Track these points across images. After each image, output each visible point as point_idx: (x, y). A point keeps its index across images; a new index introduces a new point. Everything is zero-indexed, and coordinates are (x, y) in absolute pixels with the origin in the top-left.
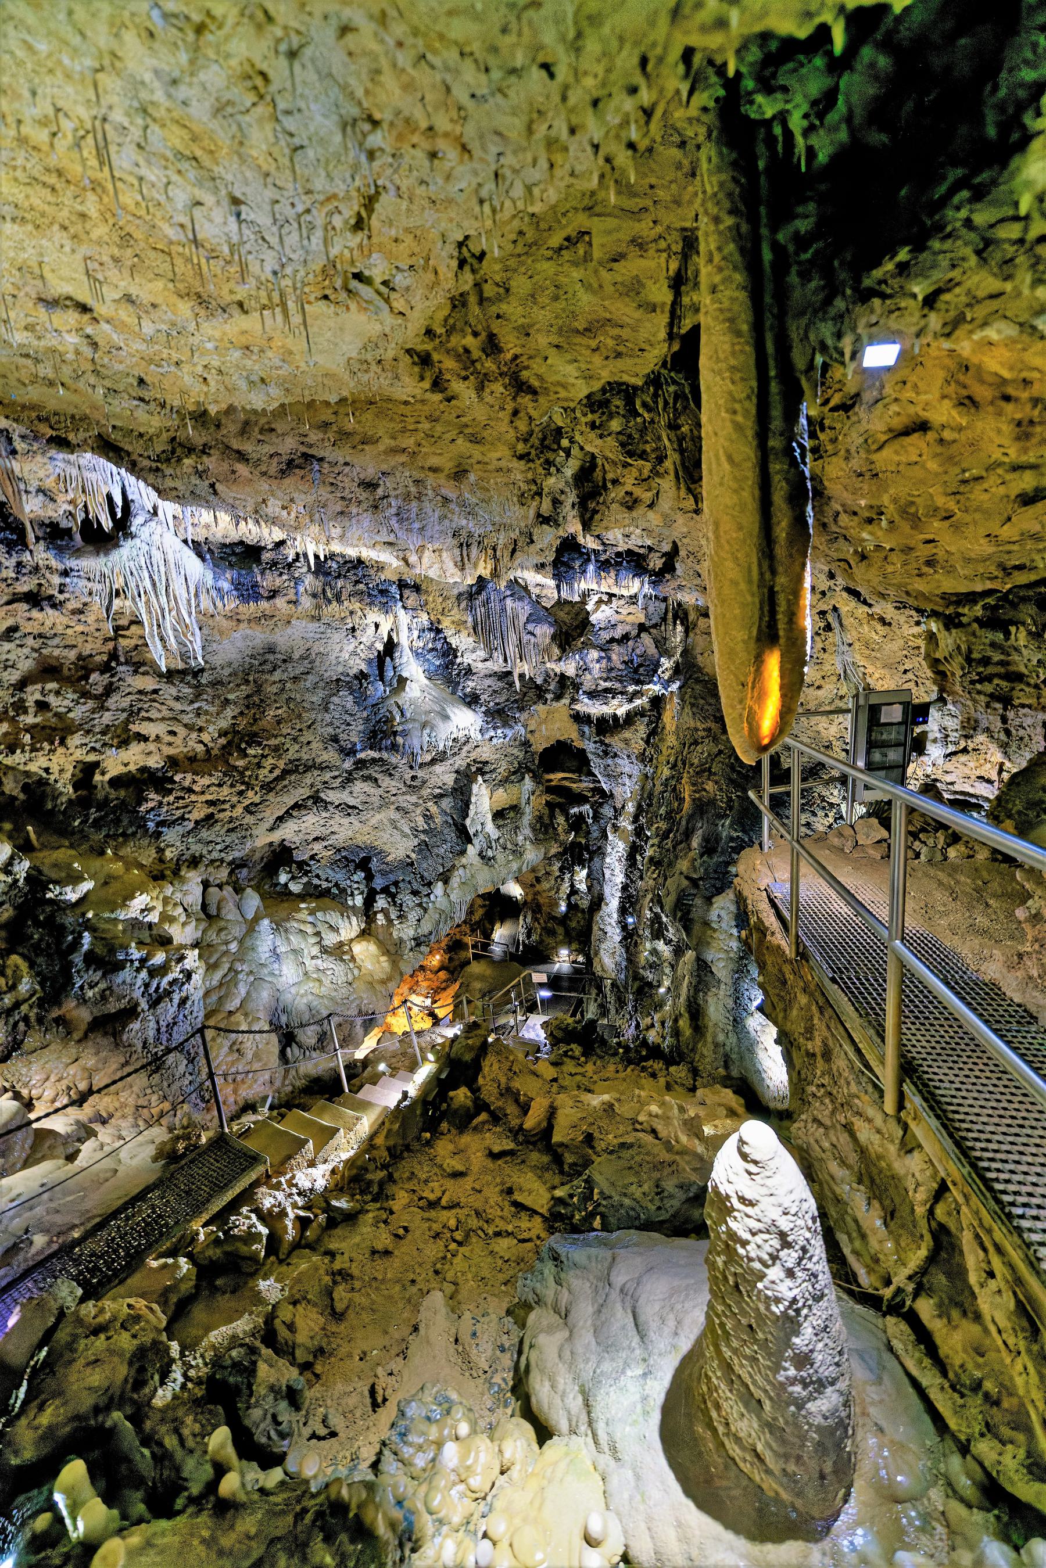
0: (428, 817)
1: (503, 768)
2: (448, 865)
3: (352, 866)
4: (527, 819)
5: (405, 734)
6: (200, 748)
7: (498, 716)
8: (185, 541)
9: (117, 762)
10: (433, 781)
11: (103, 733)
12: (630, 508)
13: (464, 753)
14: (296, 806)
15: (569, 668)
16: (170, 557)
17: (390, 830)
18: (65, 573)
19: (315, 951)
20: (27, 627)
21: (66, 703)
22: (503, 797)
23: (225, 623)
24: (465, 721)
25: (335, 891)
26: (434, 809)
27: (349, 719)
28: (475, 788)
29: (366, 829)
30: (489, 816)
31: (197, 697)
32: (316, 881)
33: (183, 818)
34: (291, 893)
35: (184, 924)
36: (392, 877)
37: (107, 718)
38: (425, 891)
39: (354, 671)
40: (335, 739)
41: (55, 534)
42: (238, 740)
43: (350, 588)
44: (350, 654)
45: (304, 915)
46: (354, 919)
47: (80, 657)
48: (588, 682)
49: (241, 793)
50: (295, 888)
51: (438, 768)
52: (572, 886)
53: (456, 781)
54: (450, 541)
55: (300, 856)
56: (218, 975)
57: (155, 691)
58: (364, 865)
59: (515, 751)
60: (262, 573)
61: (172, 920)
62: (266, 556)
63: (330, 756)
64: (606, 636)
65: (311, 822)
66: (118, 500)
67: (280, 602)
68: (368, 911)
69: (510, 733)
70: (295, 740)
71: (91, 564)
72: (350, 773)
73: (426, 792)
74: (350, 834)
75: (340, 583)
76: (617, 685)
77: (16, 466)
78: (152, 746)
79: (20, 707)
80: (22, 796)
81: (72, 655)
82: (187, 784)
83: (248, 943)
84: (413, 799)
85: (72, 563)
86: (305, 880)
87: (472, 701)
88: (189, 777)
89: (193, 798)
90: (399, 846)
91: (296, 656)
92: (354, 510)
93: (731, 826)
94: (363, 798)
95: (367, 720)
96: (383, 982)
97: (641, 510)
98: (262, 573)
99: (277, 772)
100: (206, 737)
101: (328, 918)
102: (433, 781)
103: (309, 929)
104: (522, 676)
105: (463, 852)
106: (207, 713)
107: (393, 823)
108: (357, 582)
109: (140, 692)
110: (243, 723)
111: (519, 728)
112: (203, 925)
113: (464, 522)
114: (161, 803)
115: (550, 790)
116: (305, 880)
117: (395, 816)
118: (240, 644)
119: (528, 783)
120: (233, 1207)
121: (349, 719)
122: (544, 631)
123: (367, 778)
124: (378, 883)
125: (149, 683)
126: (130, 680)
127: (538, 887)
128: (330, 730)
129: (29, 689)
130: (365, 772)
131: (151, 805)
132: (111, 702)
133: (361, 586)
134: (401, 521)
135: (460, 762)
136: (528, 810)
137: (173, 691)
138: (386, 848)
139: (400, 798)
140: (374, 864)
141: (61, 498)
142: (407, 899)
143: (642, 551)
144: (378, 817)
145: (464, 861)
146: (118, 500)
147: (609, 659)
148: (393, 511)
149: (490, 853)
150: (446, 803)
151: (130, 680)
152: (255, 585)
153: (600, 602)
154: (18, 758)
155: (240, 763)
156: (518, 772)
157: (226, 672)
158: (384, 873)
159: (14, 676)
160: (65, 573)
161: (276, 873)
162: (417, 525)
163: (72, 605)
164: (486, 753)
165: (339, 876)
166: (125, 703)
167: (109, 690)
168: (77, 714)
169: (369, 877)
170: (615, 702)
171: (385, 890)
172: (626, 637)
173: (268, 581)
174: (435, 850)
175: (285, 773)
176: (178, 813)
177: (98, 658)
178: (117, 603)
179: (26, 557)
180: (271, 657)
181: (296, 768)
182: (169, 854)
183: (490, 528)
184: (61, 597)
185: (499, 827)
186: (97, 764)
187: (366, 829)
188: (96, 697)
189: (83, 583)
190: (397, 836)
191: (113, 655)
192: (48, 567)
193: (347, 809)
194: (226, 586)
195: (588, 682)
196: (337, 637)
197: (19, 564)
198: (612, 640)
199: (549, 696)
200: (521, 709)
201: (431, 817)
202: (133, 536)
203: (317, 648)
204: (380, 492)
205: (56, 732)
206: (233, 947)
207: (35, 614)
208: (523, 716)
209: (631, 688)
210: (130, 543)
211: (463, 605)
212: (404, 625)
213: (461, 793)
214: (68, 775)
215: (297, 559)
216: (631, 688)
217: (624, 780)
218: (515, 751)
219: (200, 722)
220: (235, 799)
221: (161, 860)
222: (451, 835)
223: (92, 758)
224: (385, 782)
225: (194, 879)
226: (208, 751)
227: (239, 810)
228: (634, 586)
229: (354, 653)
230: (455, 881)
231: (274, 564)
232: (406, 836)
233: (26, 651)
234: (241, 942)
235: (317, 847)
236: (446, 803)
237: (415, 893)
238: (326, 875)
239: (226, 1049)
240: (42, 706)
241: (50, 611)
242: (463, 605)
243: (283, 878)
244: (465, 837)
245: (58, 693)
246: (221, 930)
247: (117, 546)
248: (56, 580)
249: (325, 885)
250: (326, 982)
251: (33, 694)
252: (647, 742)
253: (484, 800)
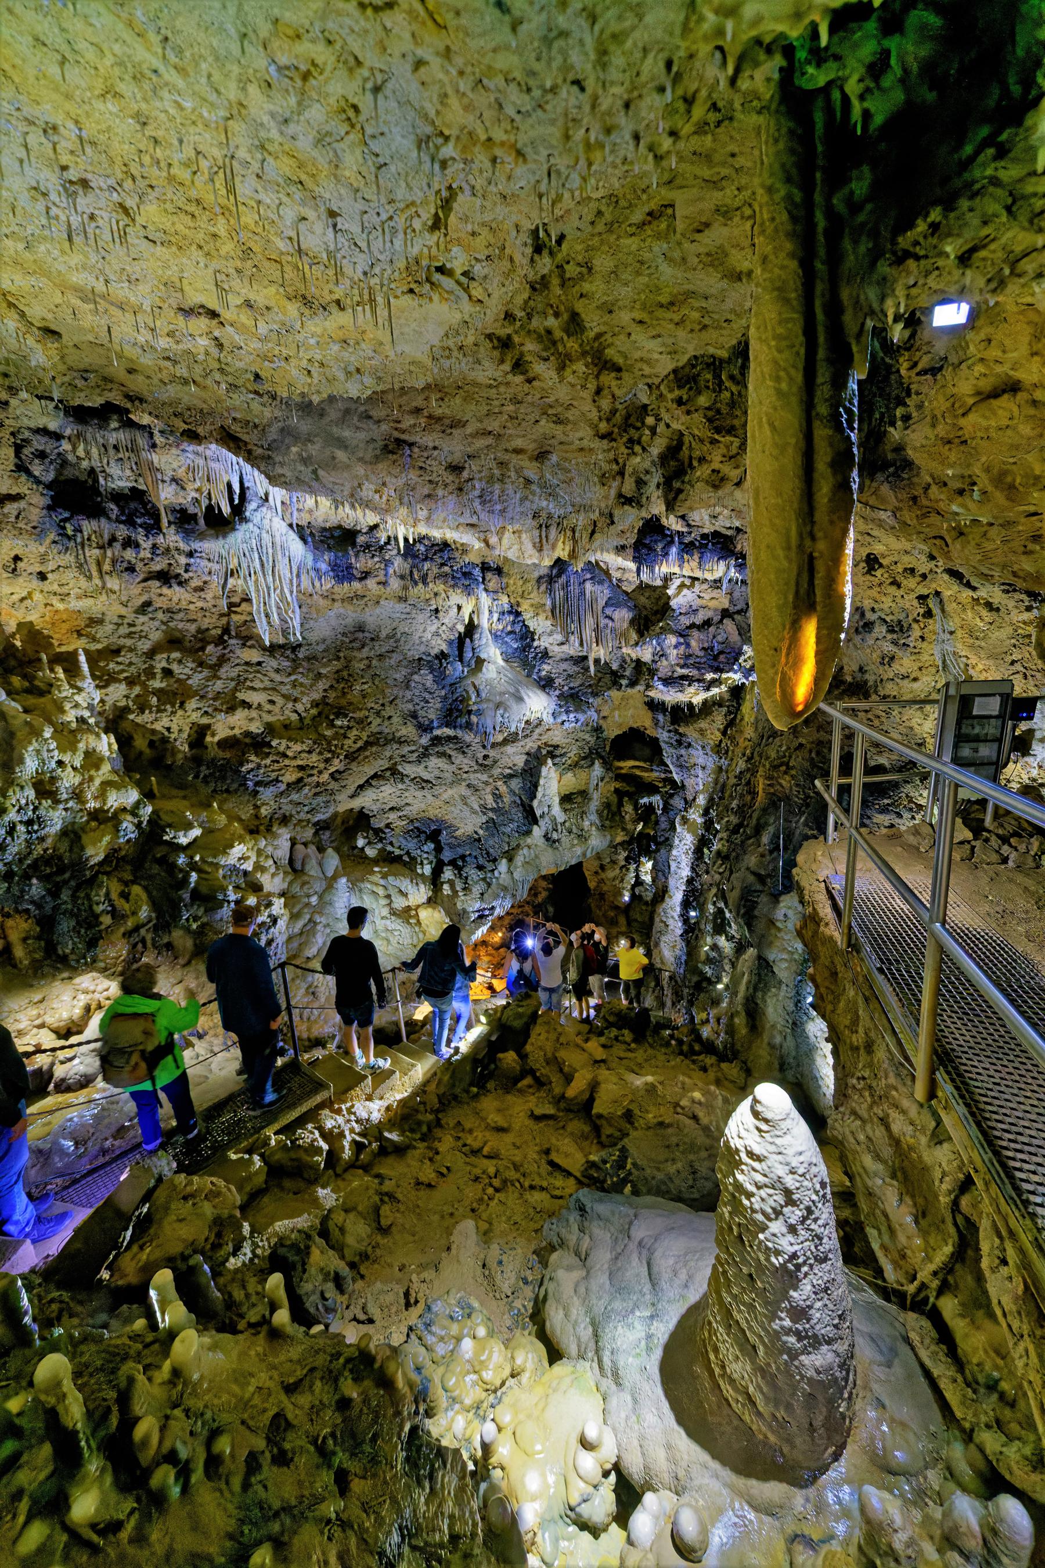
0: (497, 796)
1: (573, 753)
2: (513, 844)
3: (423, 837)
4: (595, 804)
5: (479, 713)
6: (294, 717)
7: (572, 700)
8: (291, 526)
9: (227, 726)
10: (505, 761)
11: (214, 699)
12: (716, 487)
13: (535, 736)
14: (375, 776)
15: (646, 654)
16: (278, 540)
17: (460, 805)
18: (190, 554)
19: (385, 912)
20: (159, 602)
21: (187, 671)
22: (571, 781)
23: (322, 602)
24: (538, 705)
25: (406, 858)
26: (503, 789)
27: (427, 696)
28: (544, 771)
29: (438, 803)
30: (557, 800)
31: (294, 671)
32: (389, 848)
33: (277, 781)
34: (366, 857)
35: (273, 875)
36: (460, 851)
37: (219, 685)
38: (490, 866)
39: (435, 651)
40: (414, 715)
41: (183, 519)
42: (327, 711)
43: (435, 570)
44: (432, 635)
45: (376, 878)
47: (199, 631)
48: (664, 668)
49: (327, 761)
50: (371, 852)
51: (509, 749)
52: (637, 877)
53: (527, 762)
54: (530, 522)
55: (377, 823)
56: (300, 924)
57: (259, 664)
58: (434, 836)
59: (587, 737)
60: (357, 556)
61: (264, 870)
62: (361, 539)
63: (408, 731)
64: (686, 621)
65: (386, 793)
66: (236, 488)
67: (371, 583)
68: (435, 881)
69: (582, 717)
70: (378, 714)
71: (211, 546)
72: (426, 749)
73: (496, 772)
74: (423, 806)
75: (427, 565)
76: (694, 673)
77: (155, 458)
78: (254, 714)
79: (150, 673)
80: (148, 751)
81: (193, 628)
82: (282, 749)
83: (327, 898)
84: (484, 777)
85: (196, 545)
86: (380, 846)
87: (546, 684)
88: (284, 742)
89: (287, 762)
90: (468, 823)
91: (383, 635)
92: (440, 492)
93: (806, 824)
94: (437, 773)
95: (445, 698)
97: (728, 488)
98: (357, 556)
99: (360, 744)
100: (300, 707)
101: (397, 883)
102: (505, 761)
103: (381, 891)
104: (597, 661)
105: (529, 833)
106: (301, 685)
107: (464, 798)
108: (442, 565)
109: (247, 663)
110: (332, 695)
111: (592, 714)
112: (289, 878)
113: (544, 504)
114: (259, 766)
115: (619, 777)
116: (380, 846)
117: (466, 792)
118: (334, 622)
119: (598, 769)
120: (300, 1122)
121: (427, 696)
122: (623, 616)
123: (443, 755)
124: (447, 855)
125: (253, 655)
126: (238, 652)
127: (603, 875)
128: (410, 706)
129: (158, 657)
130: (440, 749)
131: (251, 766)
132: (223, 672)
133: (446, 569)
134: (483, 503)
135: (531, 745)
136: (596, 796)
137: (274, 664)
138: (456, 823)
139: (472, 776)
140: (444, 837)
141: (190, 486)
143: (729, 533)
144: (450, 792)
145: (529, 841)
146: (236, 488)
147: (688, 645)
148: (477, 493)
149: (555, 836)
150: (516, 784)
151: (238, 652)
152: (350, 567)
153: (682, 586)
154: (147, 717)
155: (328, 733)
156: (589, 757)
157: (321, 647)
158: (452, 847)
159: (145, 646)
160: (190, 554)
161: (354, 838)
162: (498, 507)
163: (195, 583)
164: (557, 737)
165: (411, 845)
166: (234, 673)
167: (222, 660)
168: (196, 681)
169: (439, 849)
170: (692, 690)
171: (452, 863)
172: (707, 623)
173: (361, 563)
175: (368, 744)
176: (274, 775)
177: (213, 632)
178: (231, 581)
179: (160, 539)
180: (360, 635)
181: (376, 741)
182: (264, 811)
183: (570, 509)
184: (186, 576)
185: (565, 811)
186: (208, 727)
187: (438, 803)
188: (211, 667)
189: (205, 563)
190: (467, 812)
191: (226, 630)
192: (177, 549)
193: (423, 783)
194: (323, 567)
195: (664, 668)
196: (421, 617)
197: (154, 546)
198: (693, 626)
199: (624, 682)
200: (595, 695)
201: (500, 796)
202: (246, 520)
203: (403, 628)
204: (465, 474)
205: (175, 696)
206: (314, 900)
207: (165, 590)
208: (596, 702)
209: (709, 676)
210: (244, 527)
211: (543, 587)
212: (483, 607)
213: (530, 775)
214: (185, 735)
215: (388, 543)
216: (709, 676)
217: (698, 770)
218: (587, 737)
219: (296, 693)
220: (322, 766)
221: (257, 817)
222: (518, 815)
223: (205, 721)
224: (459, 759)
225: (283, 837)
226: (301, 719)
227: (325, 776)
228: (719, 569)
229: (437, 634)
230: (519, 860)
231: (367, 546)
233: (157, 623)
234: (321, 897)
235: (393, 816)
236: (516, 784)
237: (480, 868)
238: (399, 844)
239: (302, 991)
240: (167, 673)
241: (176, 588)
242: (543, 587)
243: (361, 843)
244: (531, 818)
245: (180, 662)
246: (304, 884)
247: (234, 529)
248: (183, 560)
249: (397, 852)
250: (394, 941)
251: (160, 662)
252: (724, 733)
253: (552, 783)
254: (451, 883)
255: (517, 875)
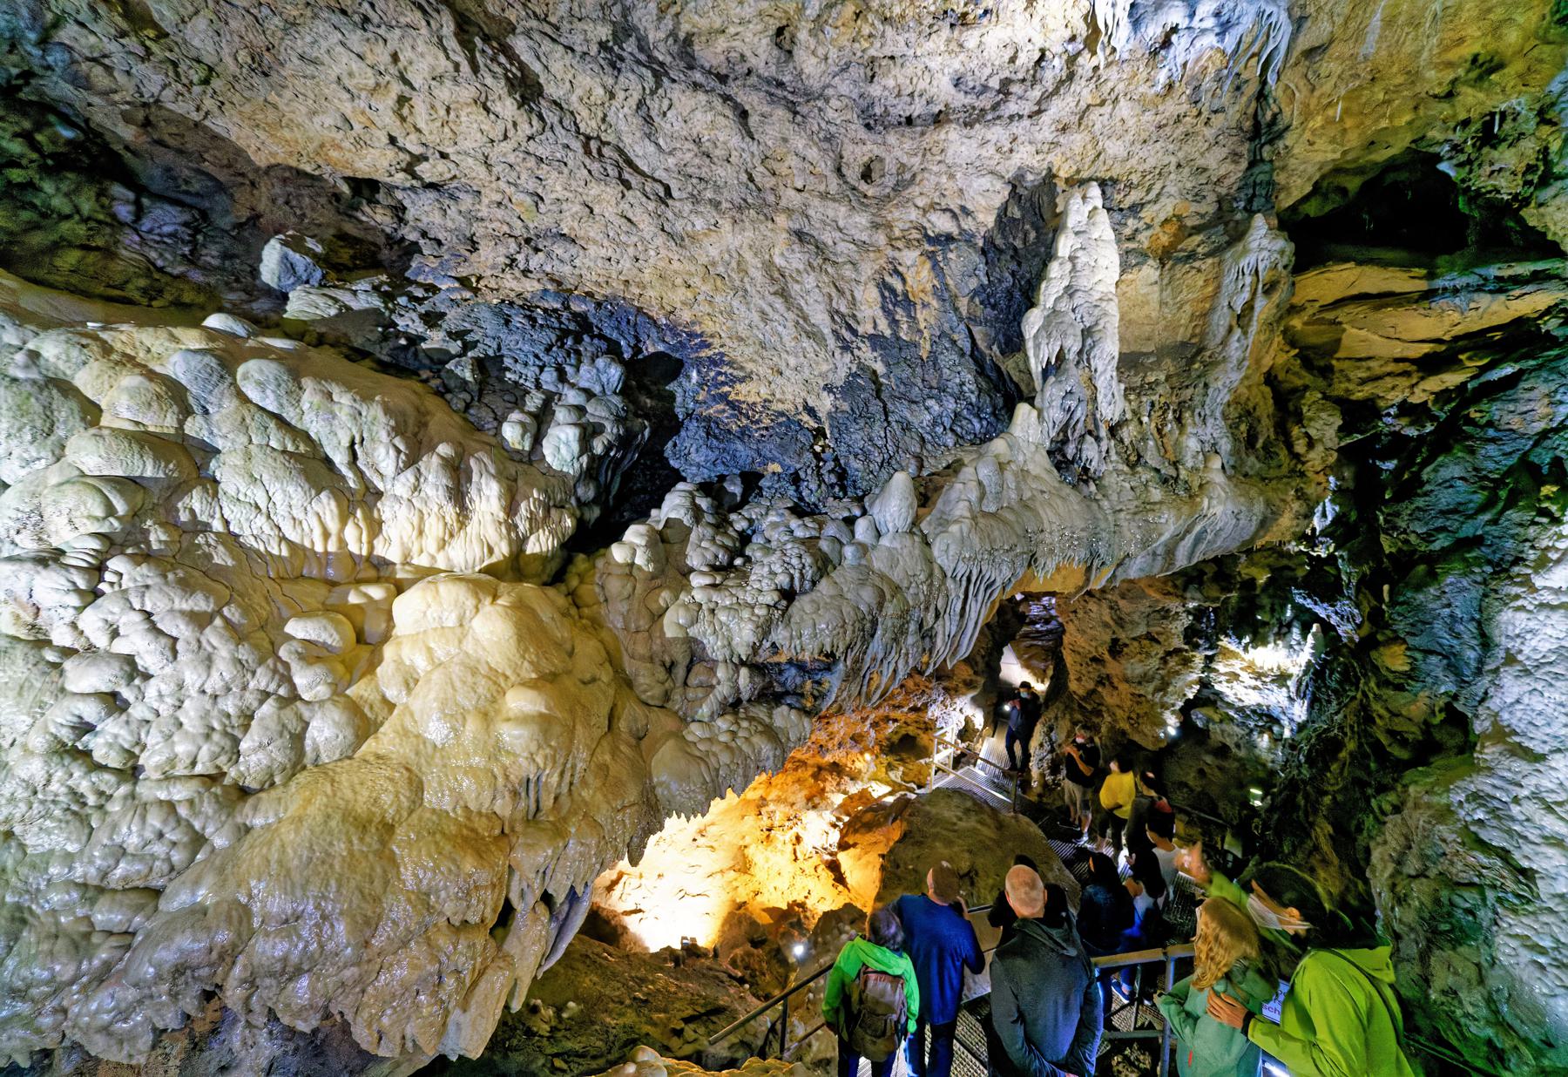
0: (896, 300)
26: (919, 277)
46: (487, 496)
51: (957, 143)
52: (1205, 684)
90: (784, 371)
96: (482, 838)
117: (792, 259)
127: (1112, 667)
138: (737, 352)
139: (817, 209)
140: (687, 390)
142: (771, 521)
150: (963, 268)
174: (901, 410)
201: (908, 303)
232: (814, 335)
254: (666, 542)
255: (945, 552)
